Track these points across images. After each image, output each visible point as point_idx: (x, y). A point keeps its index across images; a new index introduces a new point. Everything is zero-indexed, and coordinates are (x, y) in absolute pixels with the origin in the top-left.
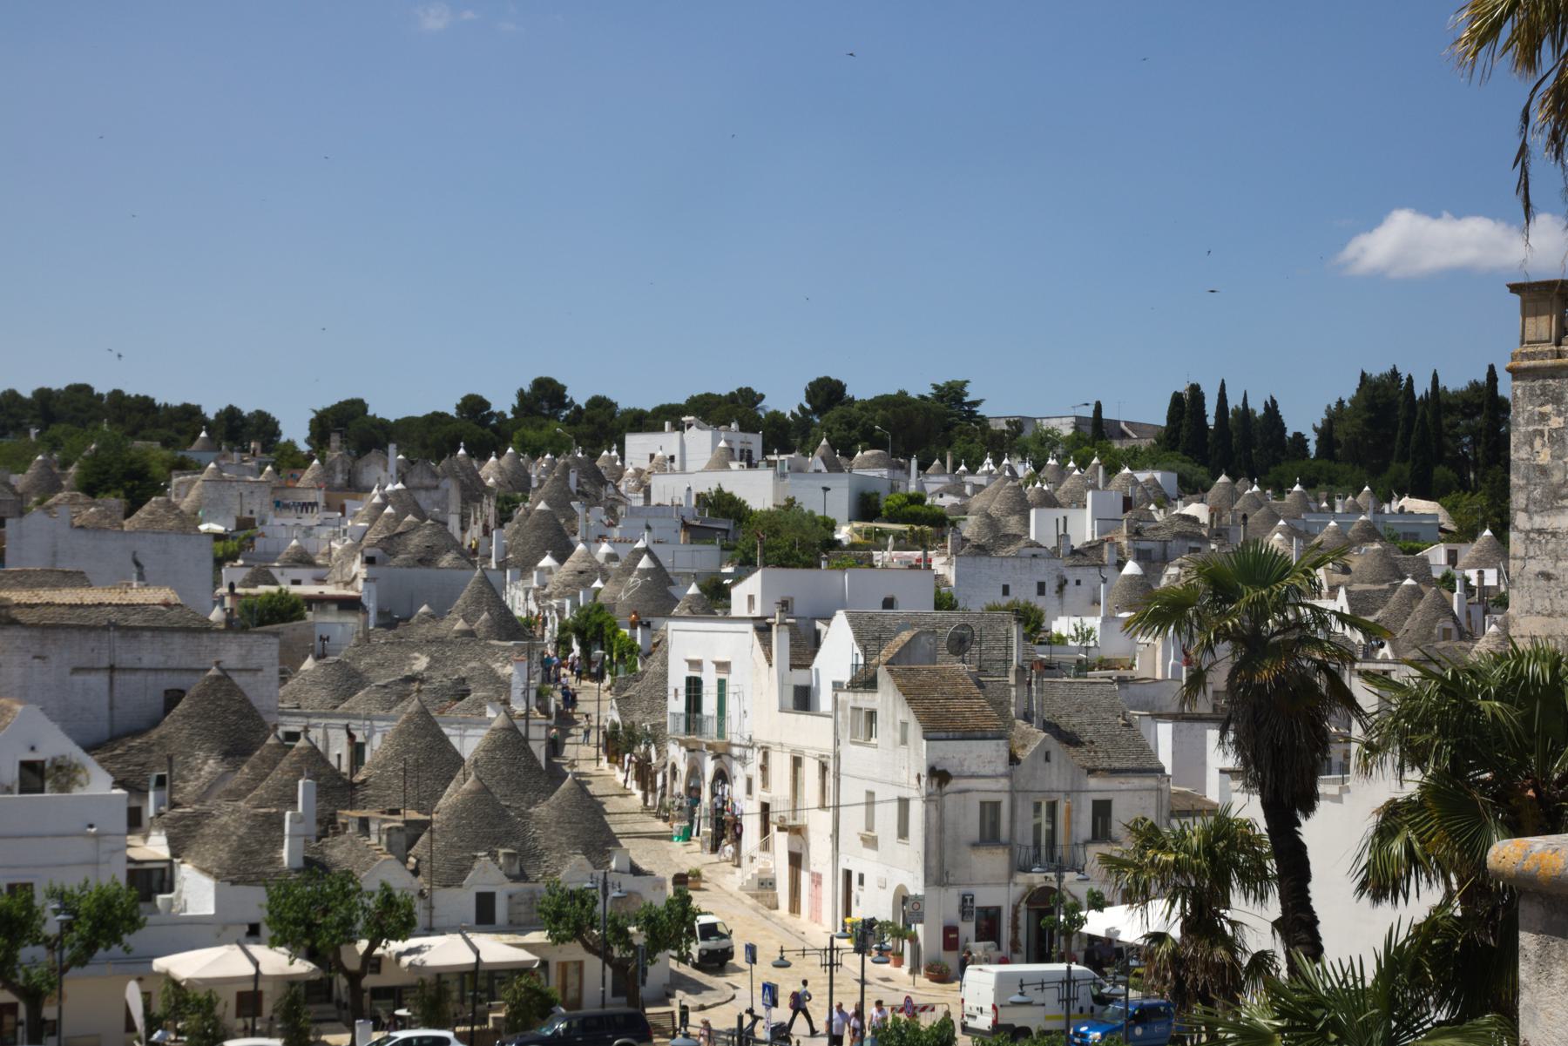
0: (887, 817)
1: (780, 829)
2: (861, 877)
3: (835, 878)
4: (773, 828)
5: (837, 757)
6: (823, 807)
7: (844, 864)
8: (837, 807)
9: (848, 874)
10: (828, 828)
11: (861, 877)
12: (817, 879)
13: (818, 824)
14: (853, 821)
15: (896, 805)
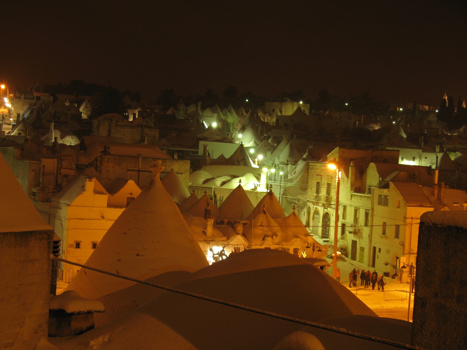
0: (391, 231)
1: (350, 232)
2: (380, 249)
3: (370, 249)
4: (347, 232)
5: (373, 209)
6: (366, 225)
7: (373, 245)
8: (372, 226)
9: (375, 248)
10: (368, 233)
11: (380, 249)
12: (362, 249)
13: (366, 231)
14: (378, 231)
15: (394, 227)
